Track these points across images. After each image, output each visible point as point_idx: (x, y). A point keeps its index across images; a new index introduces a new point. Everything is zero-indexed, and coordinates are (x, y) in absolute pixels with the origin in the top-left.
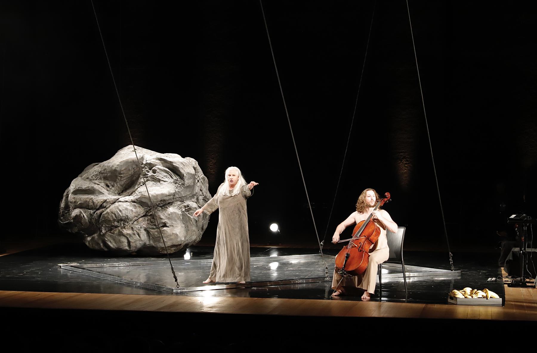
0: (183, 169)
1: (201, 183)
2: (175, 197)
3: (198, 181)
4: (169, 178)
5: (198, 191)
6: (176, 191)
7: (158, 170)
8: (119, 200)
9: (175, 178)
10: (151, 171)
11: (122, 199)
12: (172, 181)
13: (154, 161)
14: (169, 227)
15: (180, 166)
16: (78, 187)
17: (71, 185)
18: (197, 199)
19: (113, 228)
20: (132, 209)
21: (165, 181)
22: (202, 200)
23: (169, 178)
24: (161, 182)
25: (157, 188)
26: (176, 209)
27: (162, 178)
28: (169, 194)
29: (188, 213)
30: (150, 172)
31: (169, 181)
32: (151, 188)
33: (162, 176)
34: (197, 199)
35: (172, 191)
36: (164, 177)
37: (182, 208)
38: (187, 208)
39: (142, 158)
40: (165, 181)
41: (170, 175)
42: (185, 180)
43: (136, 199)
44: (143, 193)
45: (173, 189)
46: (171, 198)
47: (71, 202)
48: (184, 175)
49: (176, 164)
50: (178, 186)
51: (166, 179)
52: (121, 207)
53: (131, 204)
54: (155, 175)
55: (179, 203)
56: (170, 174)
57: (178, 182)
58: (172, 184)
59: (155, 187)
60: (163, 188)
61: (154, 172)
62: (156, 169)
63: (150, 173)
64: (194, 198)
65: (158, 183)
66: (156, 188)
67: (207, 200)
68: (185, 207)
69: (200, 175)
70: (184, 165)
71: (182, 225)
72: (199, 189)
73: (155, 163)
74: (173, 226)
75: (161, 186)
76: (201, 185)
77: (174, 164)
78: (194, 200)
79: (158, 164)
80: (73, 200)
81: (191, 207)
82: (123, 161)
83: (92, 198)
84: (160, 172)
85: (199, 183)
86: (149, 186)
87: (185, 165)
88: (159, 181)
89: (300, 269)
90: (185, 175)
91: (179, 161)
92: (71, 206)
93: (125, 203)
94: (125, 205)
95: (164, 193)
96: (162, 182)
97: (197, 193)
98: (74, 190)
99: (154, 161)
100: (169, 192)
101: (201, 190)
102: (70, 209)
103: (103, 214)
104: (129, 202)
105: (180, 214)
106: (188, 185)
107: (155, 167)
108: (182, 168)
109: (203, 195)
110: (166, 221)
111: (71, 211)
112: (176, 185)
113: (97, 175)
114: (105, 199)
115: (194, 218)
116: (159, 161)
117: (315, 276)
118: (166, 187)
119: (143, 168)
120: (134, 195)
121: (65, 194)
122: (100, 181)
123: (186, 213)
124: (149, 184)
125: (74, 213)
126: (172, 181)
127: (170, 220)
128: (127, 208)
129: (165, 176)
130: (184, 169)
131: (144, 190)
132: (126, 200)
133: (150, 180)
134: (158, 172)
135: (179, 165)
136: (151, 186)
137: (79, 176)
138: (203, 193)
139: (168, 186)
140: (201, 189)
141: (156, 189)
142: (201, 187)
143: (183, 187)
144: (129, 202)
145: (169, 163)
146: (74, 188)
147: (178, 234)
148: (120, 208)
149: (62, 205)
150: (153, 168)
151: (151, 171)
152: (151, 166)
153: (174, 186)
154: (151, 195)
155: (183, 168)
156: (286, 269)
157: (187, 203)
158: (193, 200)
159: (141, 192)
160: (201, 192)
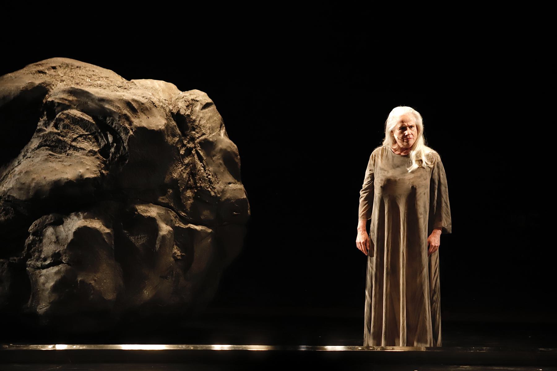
5: (181, 175)
13: (64, 96)
27: (75, 140)
31: (89, 149)
64: (164, 193)
69: (197, 136)
129: (81, 136)
130: (133, 119)
138: (195, 183)
155: (129, 114)
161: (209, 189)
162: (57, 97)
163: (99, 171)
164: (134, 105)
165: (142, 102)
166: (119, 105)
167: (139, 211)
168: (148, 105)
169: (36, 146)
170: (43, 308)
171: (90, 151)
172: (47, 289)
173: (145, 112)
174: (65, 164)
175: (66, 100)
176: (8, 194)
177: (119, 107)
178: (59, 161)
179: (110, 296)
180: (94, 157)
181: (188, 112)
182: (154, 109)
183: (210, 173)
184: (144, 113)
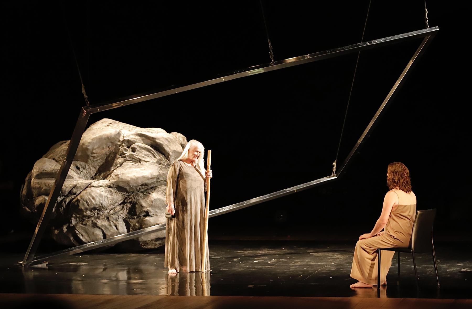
0: (168, 146)
2: (159, 180)
4: (151, 157)
6: (160, 173)
7: (138, 149)
9: (158, 157)
10: (129, 150)
11: (95, 183)
12: (155, 160)
16: (42, 170)
17: (34, 168)
20: (107, 195)
21: (146, 162)
23: (151, 157)
24: (141, 163)
25: (138, 169)
26: (160, 194)
27: (143, 157)
30: (129, 151)
32: (129, 170)
33: (143, 155)
36: (145, 156)
39: (119, 134)
40: (146, 162)
41: (153, 154)
42: (171, 159)
43: (112, 183)
45: (156, 171)
46: (154, 182)
47: (35, 188)
49: (160, 140)
51: (148, 159)
53: (106, 189)
54: (135, 155)
56: (153, 152)
57: (162, 162)
58: (155, 165)
59: (135, 168)
60: (144, 169)
61: (134, 150)
62: (135, 147)
65: (139, 164)
66: (136, 169)
74: (157, 215)
75: (141, 168)
77: (157, 141)
79: (138, 141)
80: (37, 186)
82: (96, 137)
84: (141, 151)
86: (128, 168)
87: (170, 141)
88: (140, 161)
89: (309, 263)
90: (170, 153)
91: (163, 137)
92: (35, 192)
93: (99, 188)
94: (98, 190)
95: (146, 176)
98: (38, 173)
99: (133, 137)
102: (34, 196)
104: (104, 187)
107: (134, 145)
108: (166, 145)
110: (148, 209)
111: (34, 198)
112: (160, 166)
114: (75, 184)
116: (139, 138)
117: (326, 271)
118: (148, 168)
120: (110, 179)
121: (27, 178)
124: (129, 164)
125: (38, 201)
126: (155, 160)
127: (154, 208)
128: (102, 194)
130: (169, 147)
131: (121, 173)
132: (100, 185)
133: (128, 160)
134: (138, 151)
135: (163, 141)
136: (129, 168)
137: (43, 156)
139: (150, 167)
141: (136, 171)
144: (104, 187)
146: (37, 171)
148: (93, 195)
149: (24, 192)
150: (132, 146)
151: (129, 150)
152: (129, 143)
154: (130, 178)
155: (168, 145)
156: (293, 264)
162: (130, 137)
163: (158, 172)
164: (169, 140)
168: (174, 140)
171: (152, 162)
173: (174, 143)
174: (141, 169)
175: (135, 138)
178: (138, 168)
180: (154, 165)
181: (184, 143)
182: (176, 142)
184: (173, 144)
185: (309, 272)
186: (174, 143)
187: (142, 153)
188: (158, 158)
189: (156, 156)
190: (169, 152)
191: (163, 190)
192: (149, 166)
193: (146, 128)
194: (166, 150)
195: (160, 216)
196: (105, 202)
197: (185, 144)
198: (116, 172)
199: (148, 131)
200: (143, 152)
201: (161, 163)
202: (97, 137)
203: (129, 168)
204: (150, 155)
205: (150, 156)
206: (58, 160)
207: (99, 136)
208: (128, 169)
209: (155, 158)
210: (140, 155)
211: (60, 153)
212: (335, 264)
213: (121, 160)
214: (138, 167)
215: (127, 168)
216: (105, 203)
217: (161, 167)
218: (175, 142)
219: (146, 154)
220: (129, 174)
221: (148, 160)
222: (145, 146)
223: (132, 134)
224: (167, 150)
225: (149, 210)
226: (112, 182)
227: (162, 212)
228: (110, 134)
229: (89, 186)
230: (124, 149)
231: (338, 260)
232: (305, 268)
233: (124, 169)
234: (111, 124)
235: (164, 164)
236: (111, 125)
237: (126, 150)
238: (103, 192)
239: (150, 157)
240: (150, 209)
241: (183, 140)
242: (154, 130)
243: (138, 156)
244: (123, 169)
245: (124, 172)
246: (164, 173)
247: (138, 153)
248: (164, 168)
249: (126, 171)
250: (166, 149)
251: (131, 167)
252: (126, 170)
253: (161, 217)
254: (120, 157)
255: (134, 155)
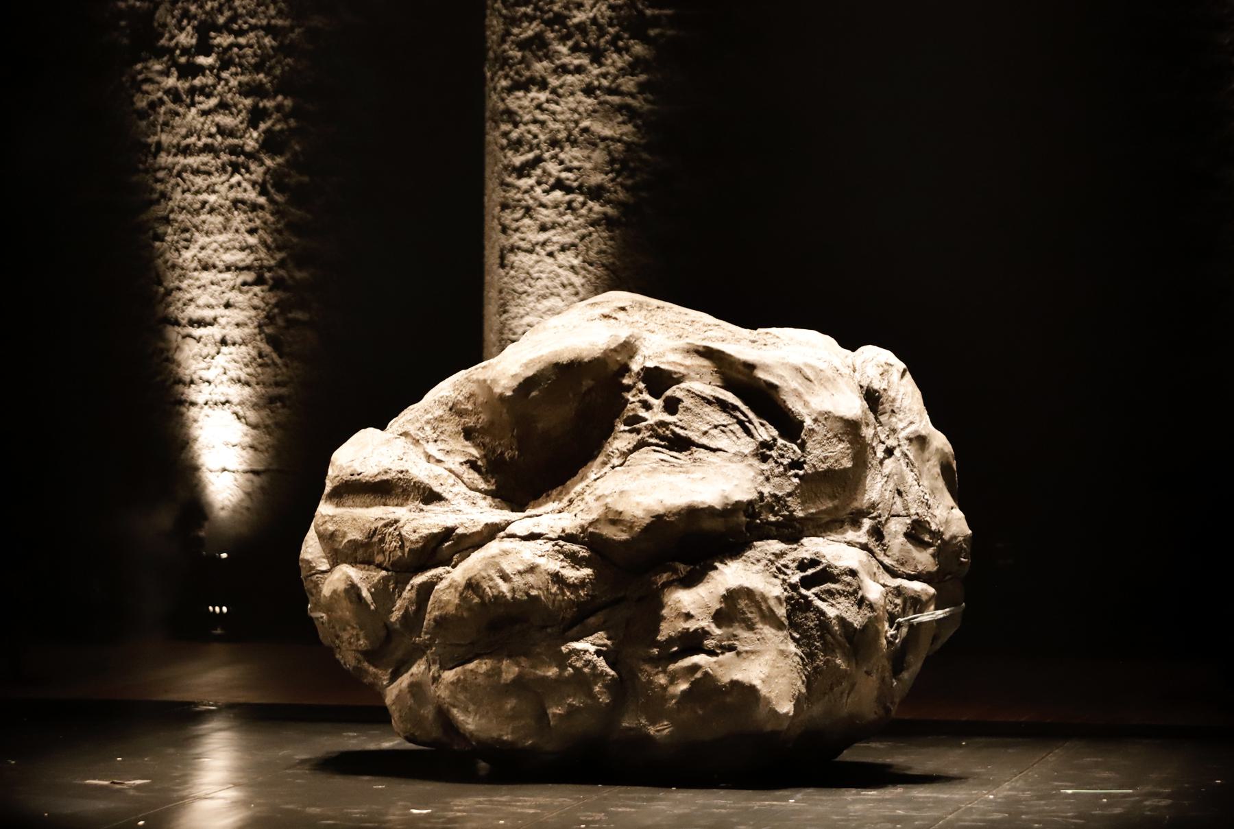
1: (903, 462)
3: (889, 452)
5: (882, 495)
6: (761, 494)
7: (688, 402)
8: (509, 530)
10: (657, 403)
11: (522, 523)
12: (748, 446)
13: (678, 358)
14: (717, 655)
15: (788, 384)
16: (349, 471)
18: (877, 533)
19: (885, 642)
20: (558, 569)
22: (902, 539)
24: (696, 455)
25: (679, 479)
26: (758, 572)
27: (705, 433)
28: (728, 504)
29: (816, 595)
30: (655, 410)
31: (733, 451)
33: (705, 428)
34: (877, 533)
35: (744, 493)
37: (789, 572)
38: (810, 572)
39: (628, 348)
41: (740, 423)
42: (809, 445)
43: (582, 527)
44: (609, 500)
45: (749, 485)
48: (802, 422)
49: (770, 373)
50: (777, 471)
52: (511, 558)
53: (557, 548)
55: (776, 546)
57: (774, 453)
58: (746, 462)
62: (679, 394)
63: (656, 415)
64: (856, 524)
66: (672, 478)
67: (927, 538)
68: (802, 565)
69: (900, 425)
70: (811, 381)
71: (782, 647)
72: (891, 486)
73: (682, 370)
75: (692, 473)
76: (902, 471)
77: (761, 374)
78: (861, 536)
79: (692, 374)
81: (829, 566)
83: (396, 521)
84: (697, 410)
85: (892, 459)
87: (812, 377)
88: (680, 444)
90: (808, 423)
91: (786, 361)
94: (529, 553)
96: (700, 454)
97: (873, 506)
99: (678, 358)
100: (726, 497)
101: (900, 493)
103: (436, 587)
104: (551, 539)
105: (778, 598)
106: (825, 466)
107: (674, 388)
108: (795, 390)
109: (908, 515)
112: (765, 466)
113: (440, 419)
114: (450, 524)
115: (844, 615)
116: (706, 363)
119: (629, 388)
122: (448, 448)
123: (803, 591)
124: (648, 457)
126: (748, 446)
128: (538, 566)
129: (716, 427)
130: (807, 397)
132: (537, 530)
134: (687, 409)
135: (782, 377)
138: (906, 508)
139: (724, 470)
140: (902, 489)
142: (902, 478)
143: (796, 475)
144: (551, 539)
145: (741, 368)
147: (759, 687)
150: (669, 393)
151: (657, 403)
152: (658, 380)
153: (752, 474)
154: (644, 510)
155: (801, 389)
157: (812, 546)
158: (851, 535)
159: (604, 495)
160: (898, 500)
161: (928, 519)
162: (664, 360)
163: (756, 488)
165: (821, 368)
166: (783, 374)
167: (828, 557)
168: (829, 373)
169: (630, 446)
170: (664, 729)
171: (735, 454)
172: (673, 697)
173: (826, 384)
174: (692, 476)
176: (591, 530)
177: (783, 376)
178: (680, 472)
179: (786, 708)
180: (741, 465)
181: (884, 386)
182: (839, 380)
183: (926, 491)
184: (825, 387)
185: (916, 823)
186: (826, 384)
187: (701, 417)
188: (760, 439)
189: (754, 431)
190: (802, 416)
191: (772, 557)
192: (720, 466)
193: (760, 330)
194: (790, 410)
195: (747, 652)
196: (551, 593)
197: (885, 390)
198: (604, 487)
199: (753, 338)
200: (705, 417)
201: (771, 456)
202: (542, 356)
203: (646, 474)
204: (731, 427)
205: (732, 431)
206: (418, 438)
207: (550, 352)
208: (642, 476)
209: (748, 439)
210: (692, 428)
211: (427, 413)
212: (999, 800)
213: (626, 444)
214: (681, 469)
215: (639, 472)
216: (551, 597)
217: (769, 472)
218: (835, 380)
219: (716, 423)
220: (641, 494)
221: (720, 446)
222: (717, 395)
223: (675, 350)
224: (793, 409)
225: (707, 629)
226: (583, 522)
227: (758, 640)
228: (589, 347)
229: (492, 532)
230: (640, 401)
231: (1008, 787)
232: (900, 809)
233: (630, 475)
234: (623, 309)
235: (779, 460)
236: (621, 315)
237: (647, 406)
238: (544, 556)
239: (731, 434)
240: (709, 626)
241: (882, 374)
242: (778, 337)
243: (686, 429)
244: (625, 476)
245: (626, 488)
246: (780, 494)
247: (685, 418)
248: (780, 475)
249: (637, 482)
250: (790, 407)
251: (655, 469)
252: (635, 479)
253: (753, 657)
254: (625, 431)
255: (670, 424)
